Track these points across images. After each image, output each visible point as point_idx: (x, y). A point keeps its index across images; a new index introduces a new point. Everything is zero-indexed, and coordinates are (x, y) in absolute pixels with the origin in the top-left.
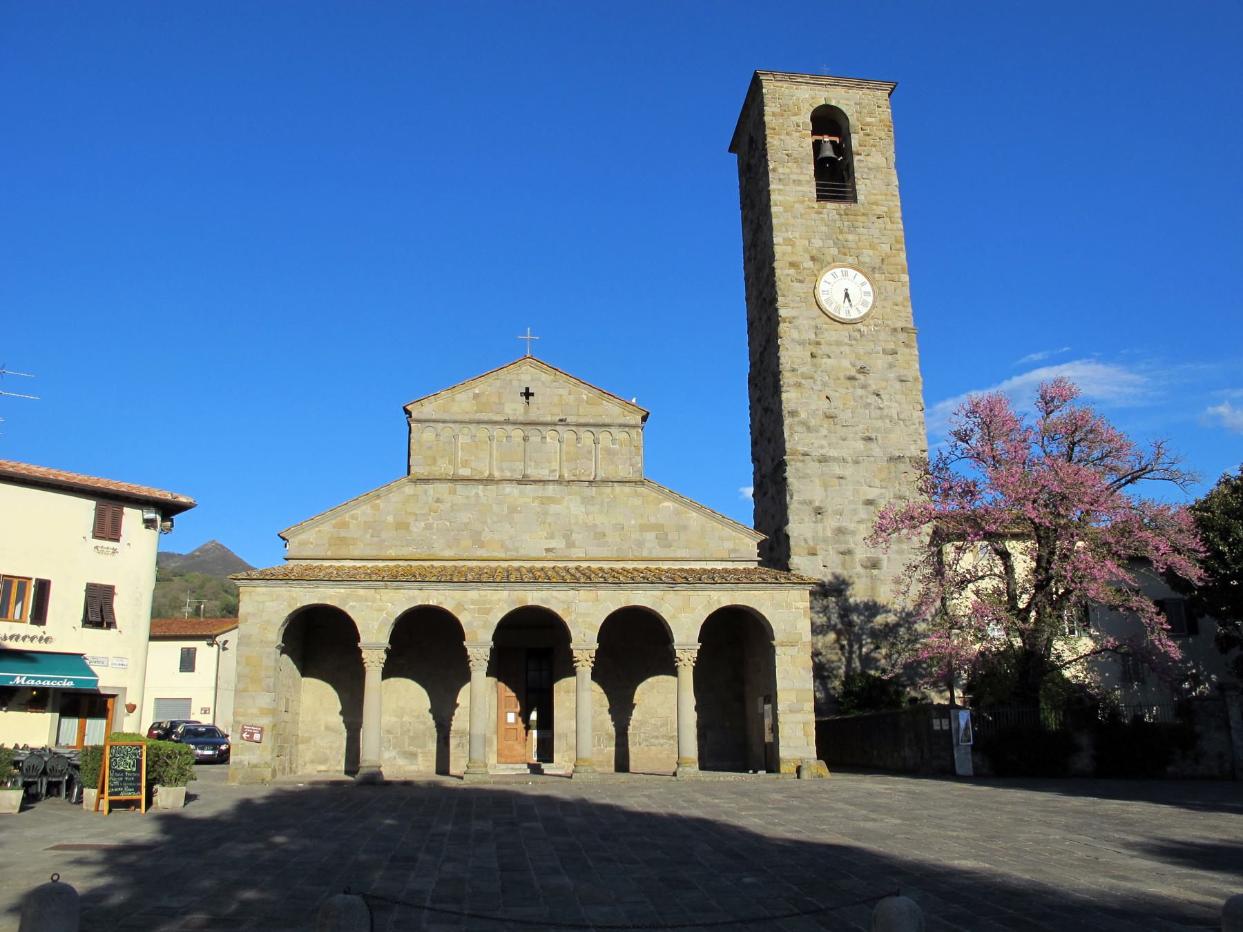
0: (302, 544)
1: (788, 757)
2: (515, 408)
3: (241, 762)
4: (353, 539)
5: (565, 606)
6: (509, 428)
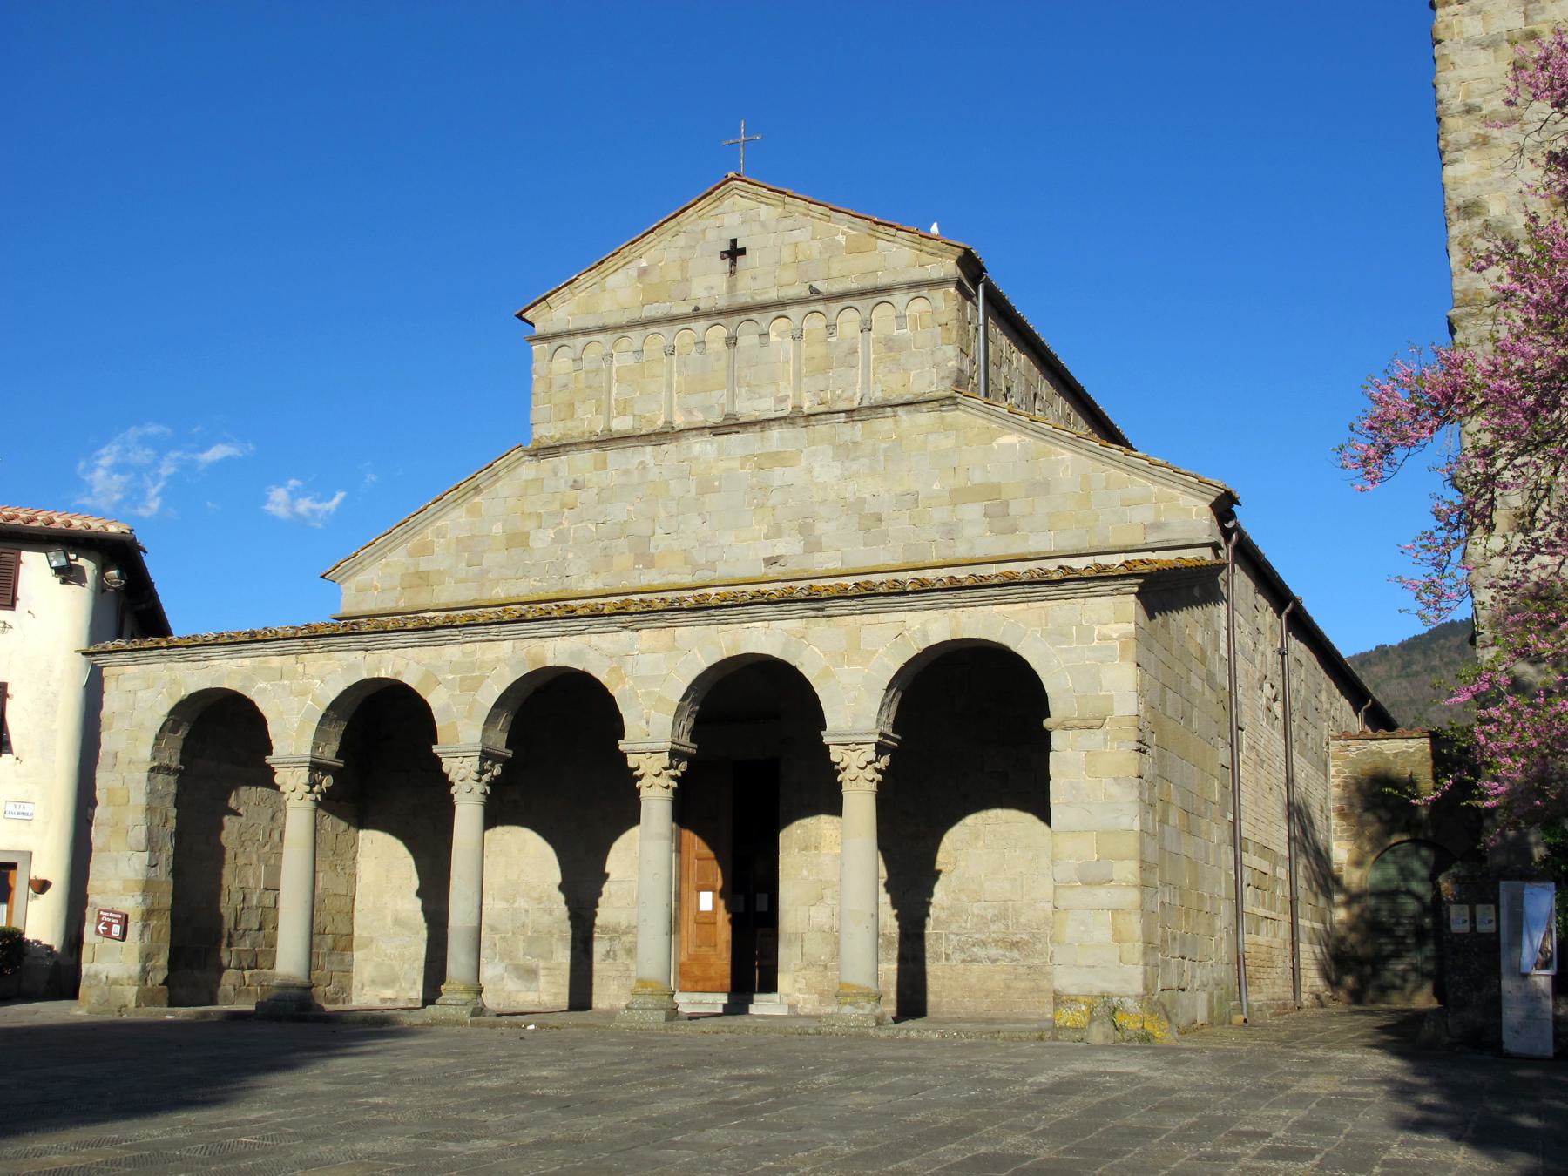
0: (359, 590)
1: (1073, 991)
2: (710, 285)
3: (96, 975)
4: (439, 572)
5: (614, 665)
6: (700, 325)
